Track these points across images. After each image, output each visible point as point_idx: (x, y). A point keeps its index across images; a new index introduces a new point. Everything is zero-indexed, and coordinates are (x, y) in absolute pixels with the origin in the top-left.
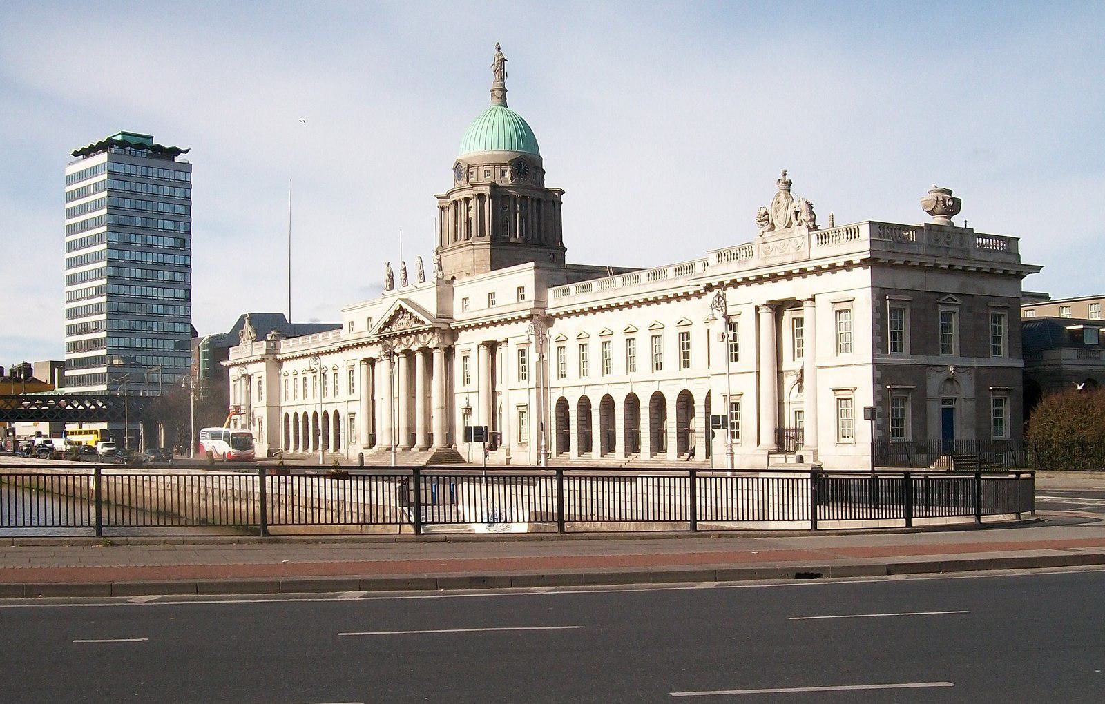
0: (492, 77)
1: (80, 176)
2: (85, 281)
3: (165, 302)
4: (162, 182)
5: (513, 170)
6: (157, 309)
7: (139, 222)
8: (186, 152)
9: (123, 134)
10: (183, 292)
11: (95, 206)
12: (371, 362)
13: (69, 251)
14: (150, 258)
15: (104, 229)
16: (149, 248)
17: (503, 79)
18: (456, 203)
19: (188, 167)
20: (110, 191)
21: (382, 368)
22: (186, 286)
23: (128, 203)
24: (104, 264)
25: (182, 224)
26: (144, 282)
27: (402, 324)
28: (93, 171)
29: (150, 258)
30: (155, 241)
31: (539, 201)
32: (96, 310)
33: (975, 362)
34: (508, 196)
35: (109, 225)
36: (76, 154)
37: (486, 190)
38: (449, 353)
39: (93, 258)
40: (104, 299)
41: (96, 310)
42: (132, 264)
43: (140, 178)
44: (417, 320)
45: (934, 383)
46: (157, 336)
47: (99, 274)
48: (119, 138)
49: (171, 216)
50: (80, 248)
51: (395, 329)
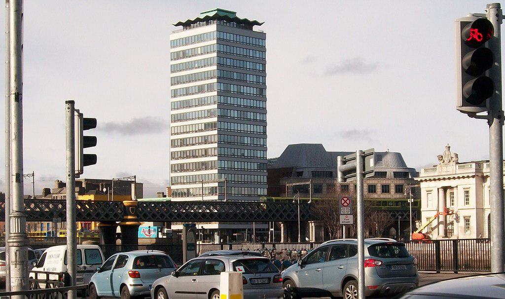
1: (186, 41)
2: (192, 119)
3: (252, 135)
6: (247, 140)
7: (235, 76)
9: (218, 10)
10: (262, 127)
11: (207, 63)
13: (175, 96)
15: (215, 80)
16: (240, 95)
19: (262, 36)
20: (219, 52)
22: (263, 123)
24: (215, 106)
25: (261, 78)
28: (199, 38)
30: (245, 90)
32: (206, 141)
35: (219, 78)
36: (179, 24)
39: (201, 102)
40: (216, 132)
41: (206, 141)
42: (232, 107)
46: (248, 160)
47: (210, 114)
50: (187, 94)
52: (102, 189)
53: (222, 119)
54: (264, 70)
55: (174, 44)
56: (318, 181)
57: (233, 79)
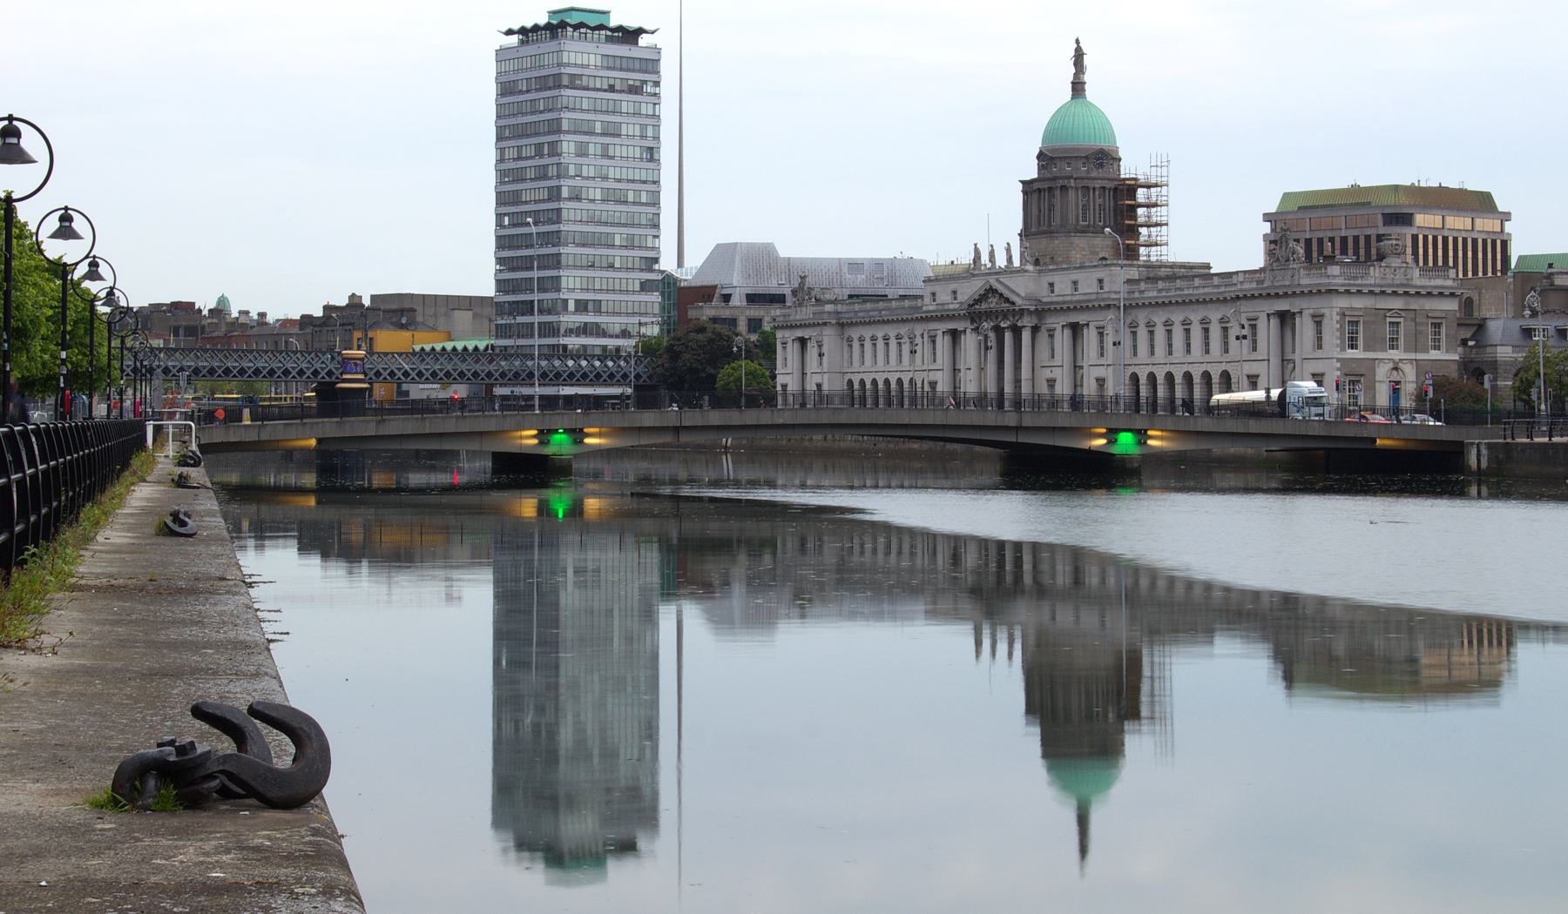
12: (955, 335)
18: (1039, 190)
21: (970, 342)
27: (993, 303)
33: (1412, 356)
38: (1035, 330)
44: (1007, 300)
45: (1382, 372)
51: (984, 306)
56: (756, 312)
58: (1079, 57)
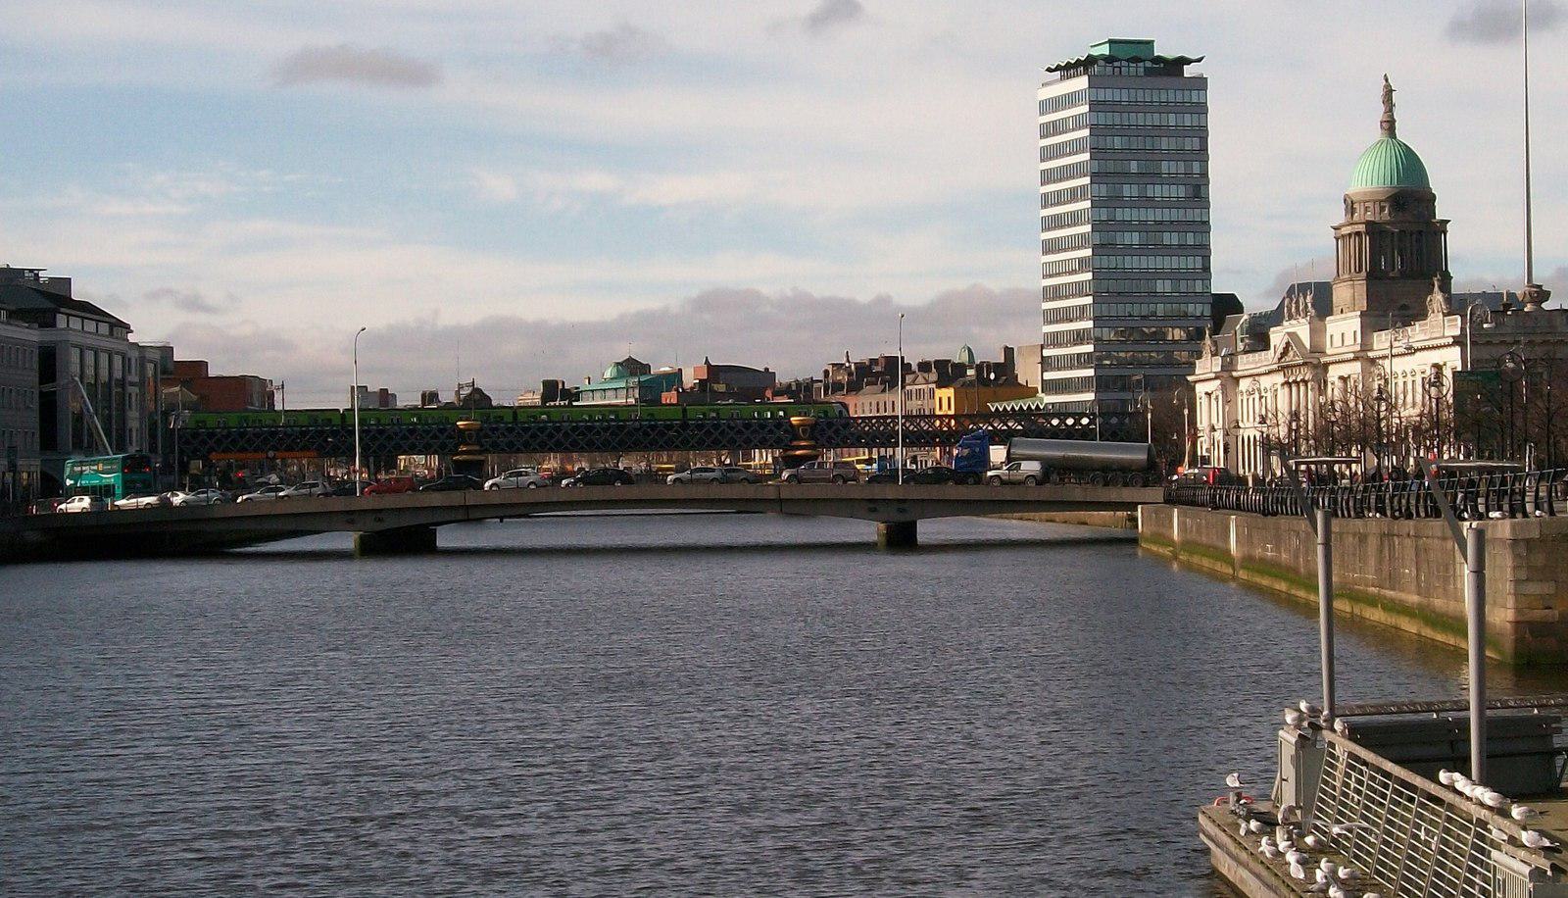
0: (1382, 108)
3: (1174, 275)
4: (1166, 107)
5: (1390, 206)
7: (1134, 167)
8: (1199, 60)
9: (1111, 42)
11: (1074, 148)
13: (1044, 206)
14: (1151, 215)
15: (1087, 180)
16: (1148, 202)
17: (1391, 110)
19: (1200, 83)
20: (1093, 128)
23: (1118, 142)
24: (1088, 228)
26: (1143, 250)
29: (1151, 215)
30: (1156, 191)
31: (1420, 232)
32: (1078, 290)
34: (1386, 232)
35: (1093, 175)
37: (1362, 228)
39: (1074, 219)
40: (1089, 276)
41: (1078, 290)
42: (1126, 226)
43: (1134, 106)
48: (1105, 50)
49: (1180, 155)
52: (988, 375)
53: (1100, 251)
54: (1204, 149)
55: (1046, 106)
57: (1127, 174)
58: (1389, 92)
